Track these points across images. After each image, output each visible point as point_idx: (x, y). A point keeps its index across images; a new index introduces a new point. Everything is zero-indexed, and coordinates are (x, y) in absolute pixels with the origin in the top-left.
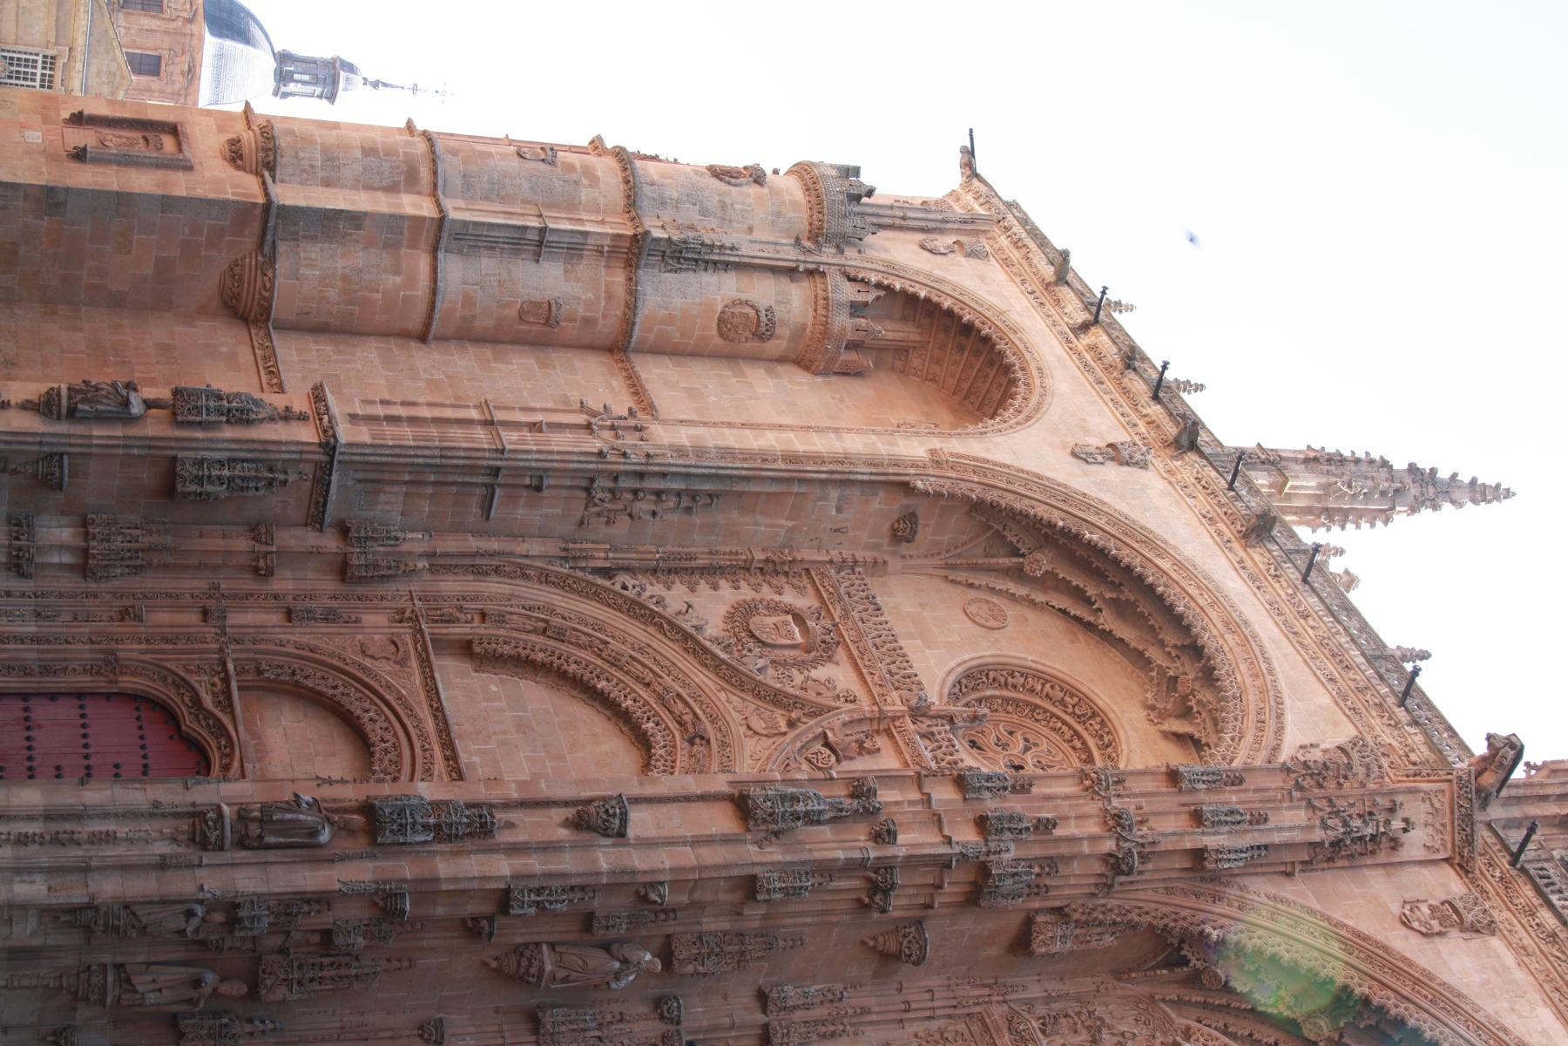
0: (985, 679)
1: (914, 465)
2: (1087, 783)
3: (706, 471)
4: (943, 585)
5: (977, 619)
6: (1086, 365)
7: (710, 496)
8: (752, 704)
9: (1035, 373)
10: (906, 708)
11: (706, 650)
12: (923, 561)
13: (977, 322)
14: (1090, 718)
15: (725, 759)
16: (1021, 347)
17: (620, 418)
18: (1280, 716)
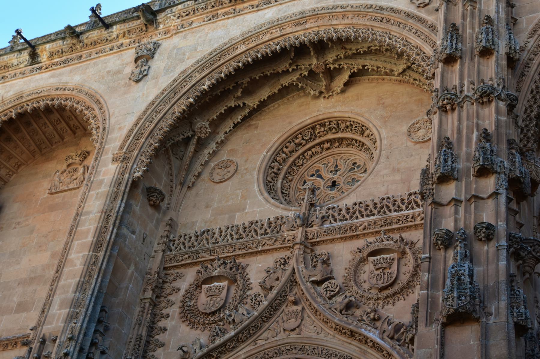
0: (271, 184)
1: (123, 174)
2: (448, 107)
3: (92, 304)
4: (193, 191)
5: (226, 177)
6: (64, 62)
7: (102, 311)
8: (272, 324)
9: (58, 92)
10: (301, 229)
11: (224, 344)
12: (174, 198)
13: (19, 111)
14: (314, 131)
15: (316, 351)
16: (34, 96)
17: (30, 352)
18: (382, 9)
